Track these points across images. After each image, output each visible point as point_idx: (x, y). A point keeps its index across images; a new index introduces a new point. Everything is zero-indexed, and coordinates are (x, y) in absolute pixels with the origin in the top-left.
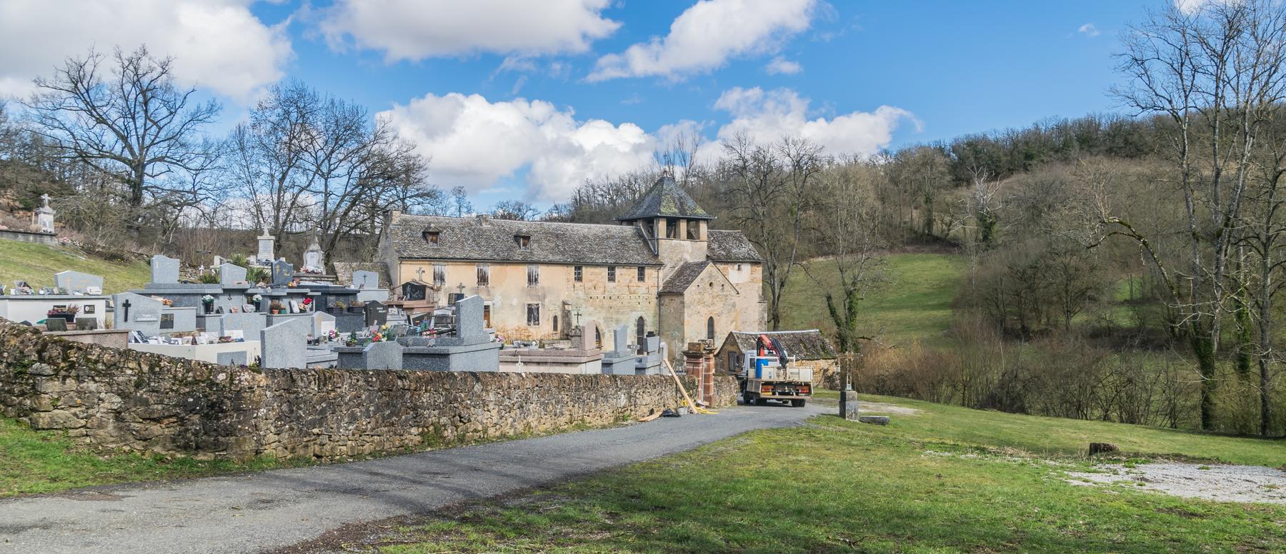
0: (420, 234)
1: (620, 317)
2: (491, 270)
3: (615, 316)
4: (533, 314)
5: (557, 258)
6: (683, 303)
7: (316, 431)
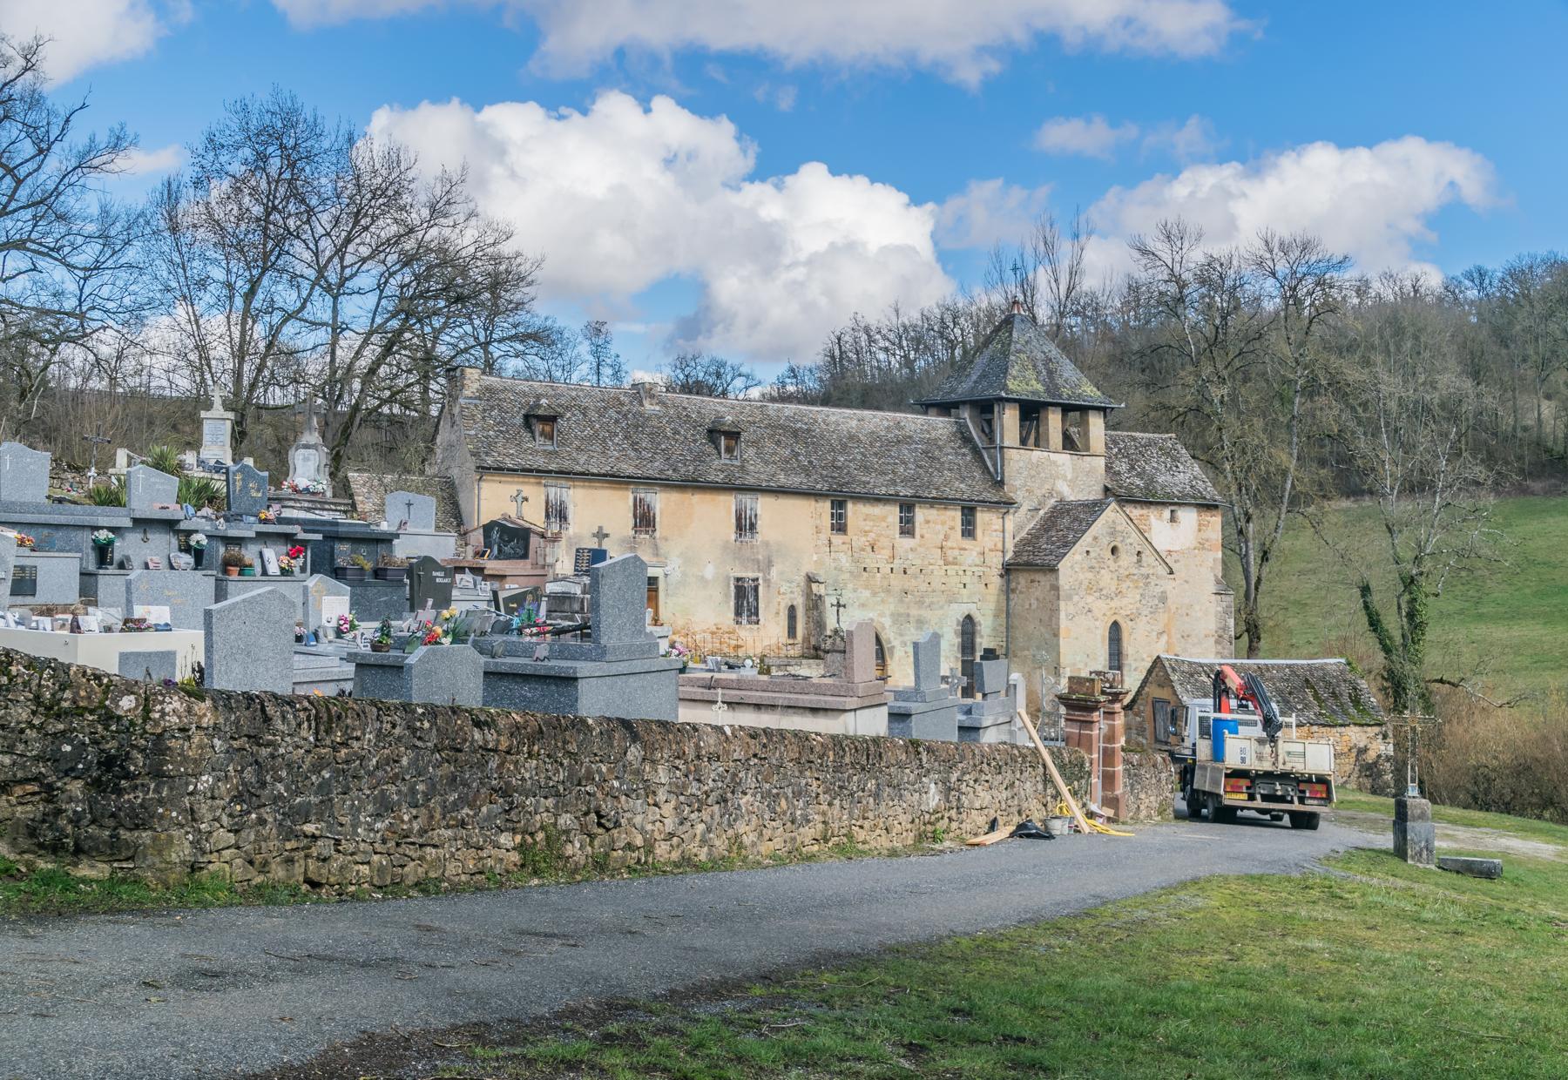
0: (519, 420)
2: (661, 502)
5: (796, 480)
6: (1056, 588)
7: (310, 828)
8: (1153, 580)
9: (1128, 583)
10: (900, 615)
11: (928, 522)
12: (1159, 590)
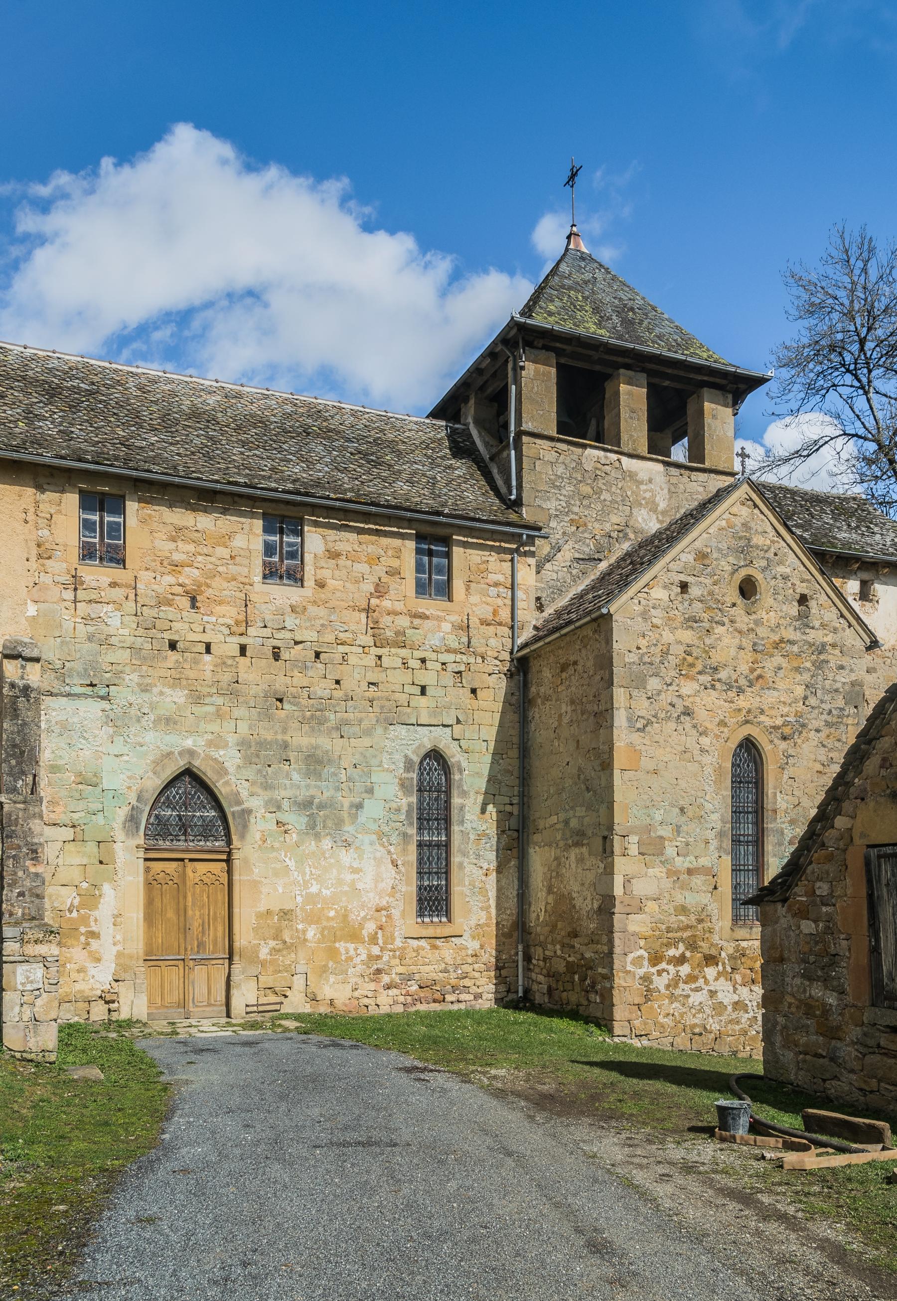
9: (778, 660)
10: (262, 744)
11: (334, 555)
12: (844, 678)
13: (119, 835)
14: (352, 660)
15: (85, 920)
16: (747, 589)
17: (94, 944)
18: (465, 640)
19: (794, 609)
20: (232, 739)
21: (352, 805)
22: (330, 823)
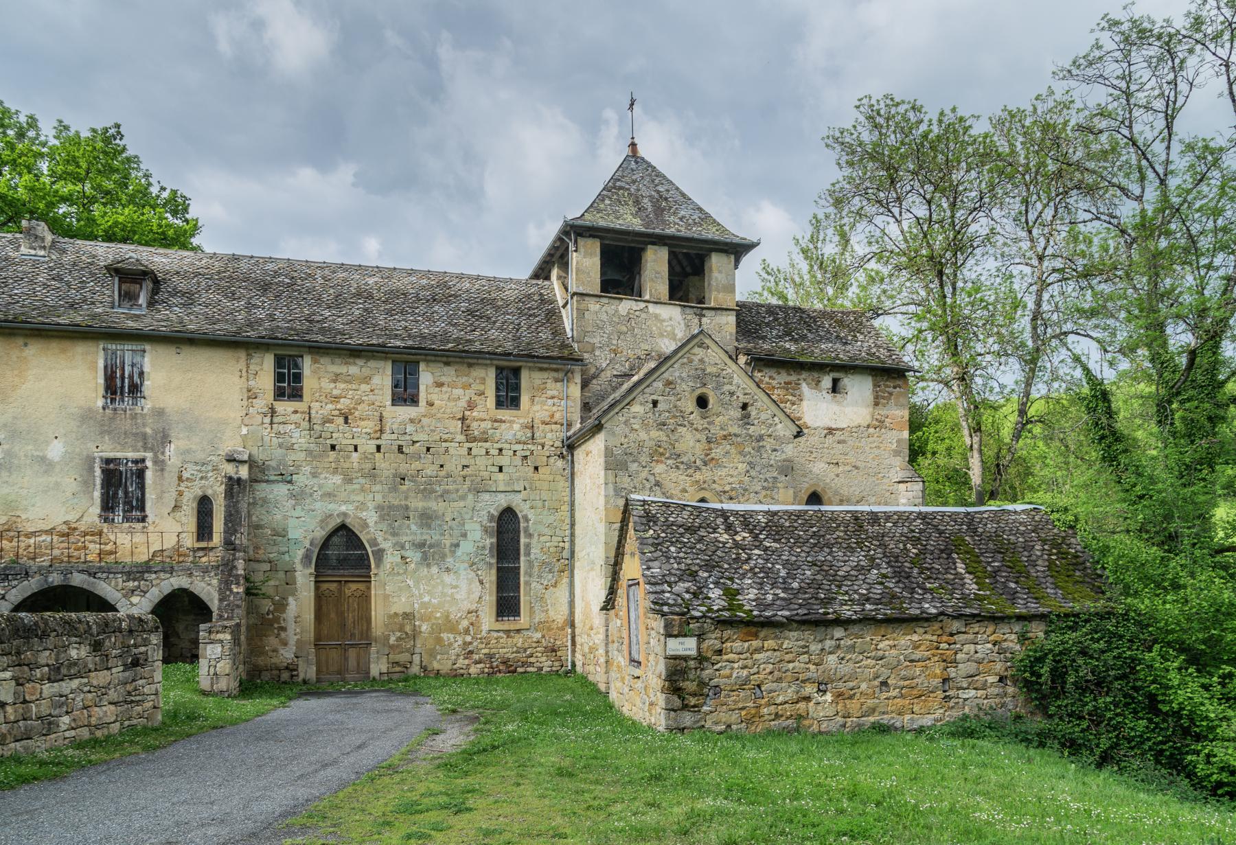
1: (435, 505)
3: (417, 504)
4: (121, 489)
8: (768, 444)
12: (780, 456)
13: (299, 567)
14: (452, 451)
15: (277, 620)
16: (702, 402)
17: (283, 635)
18: (529, 435)
19: (737, 413)
20: (371, 505)
21: (452, 545)
22: (437, 557)
